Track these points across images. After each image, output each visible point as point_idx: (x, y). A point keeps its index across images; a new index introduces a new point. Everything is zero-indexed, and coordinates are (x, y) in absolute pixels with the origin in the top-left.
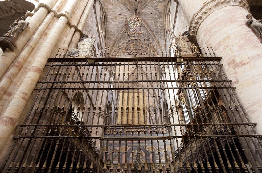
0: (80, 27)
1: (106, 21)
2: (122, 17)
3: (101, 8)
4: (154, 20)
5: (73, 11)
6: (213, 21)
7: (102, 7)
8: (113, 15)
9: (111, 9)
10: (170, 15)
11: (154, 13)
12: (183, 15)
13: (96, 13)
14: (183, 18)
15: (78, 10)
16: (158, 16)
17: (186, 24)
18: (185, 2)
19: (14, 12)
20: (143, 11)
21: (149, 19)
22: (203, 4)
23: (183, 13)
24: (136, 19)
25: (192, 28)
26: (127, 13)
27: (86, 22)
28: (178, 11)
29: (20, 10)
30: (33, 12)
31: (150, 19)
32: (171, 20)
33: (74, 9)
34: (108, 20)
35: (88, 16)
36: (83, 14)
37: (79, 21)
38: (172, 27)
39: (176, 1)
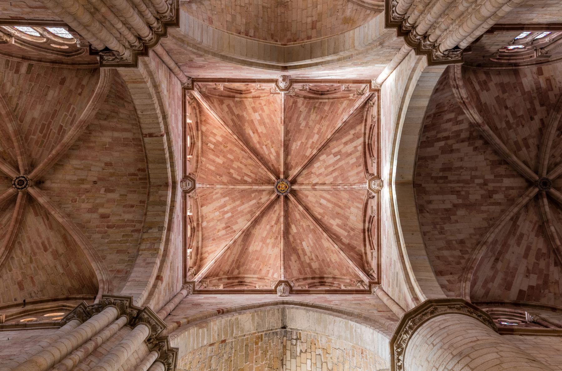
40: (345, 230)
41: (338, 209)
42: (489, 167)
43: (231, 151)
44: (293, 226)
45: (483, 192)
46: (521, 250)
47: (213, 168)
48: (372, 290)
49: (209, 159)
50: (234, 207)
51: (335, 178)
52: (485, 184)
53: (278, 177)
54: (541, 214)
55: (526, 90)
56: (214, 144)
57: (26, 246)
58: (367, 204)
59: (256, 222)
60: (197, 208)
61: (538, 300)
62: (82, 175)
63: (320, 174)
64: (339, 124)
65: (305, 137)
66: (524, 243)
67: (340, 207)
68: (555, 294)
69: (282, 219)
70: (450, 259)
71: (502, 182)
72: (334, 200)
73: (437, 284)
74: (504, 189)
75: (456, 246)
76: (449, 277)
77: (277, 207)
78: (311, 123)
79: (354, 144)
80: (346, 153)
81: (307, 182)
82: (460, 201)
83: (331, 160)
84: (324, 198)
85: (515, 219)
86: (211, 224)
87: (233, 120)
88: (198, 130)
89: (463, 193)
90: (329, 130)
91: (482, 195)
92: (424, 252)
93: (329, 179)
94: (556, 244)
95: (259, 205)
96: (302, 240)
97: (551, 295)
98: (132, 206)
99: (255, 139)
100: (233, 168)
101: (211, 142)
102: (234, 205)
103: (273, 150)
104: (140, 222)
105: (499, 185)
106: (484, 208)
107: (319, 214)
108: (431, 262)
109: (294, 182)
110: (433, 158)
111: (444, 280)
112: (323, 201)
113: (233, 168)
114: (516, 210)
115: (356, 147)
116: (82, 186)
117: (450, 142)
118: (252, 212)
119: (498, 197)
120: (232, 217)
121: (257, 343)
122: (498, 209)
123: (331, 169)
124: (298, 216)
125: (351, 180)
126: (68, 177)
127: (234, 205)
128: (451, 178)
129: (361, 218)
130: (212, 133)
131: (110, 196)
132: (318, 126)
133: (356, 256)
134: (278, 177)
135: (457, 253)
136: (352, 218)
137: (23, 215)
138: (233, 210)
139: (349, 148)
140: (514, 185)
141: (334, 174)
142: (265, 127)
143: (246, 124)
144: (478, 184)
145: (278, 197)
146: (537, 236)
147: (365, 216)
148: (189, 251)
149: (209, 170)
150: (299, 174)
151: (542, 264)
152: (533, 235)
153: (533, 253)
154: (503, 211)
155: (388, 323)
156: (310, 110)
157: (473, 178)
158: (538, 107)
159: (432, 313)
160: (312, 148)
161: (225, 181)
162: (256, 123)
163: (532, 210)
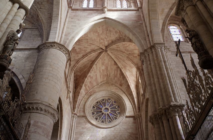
6: (43, 123)
42: (111, 39)
45: (103, 38)
46: (86, 46)
52: (106, 38)
55: (134, 51)
66: (88, 47)
68: (75, 56)
71: (106, 41)
74: (104, 42)
82: (100, 34)
89: (103, 34)
91: (102, 38)
94: (88, 55)
97: (74, 55)
105: (106, 41)
106: (98, 38)
110: (114, 29)
117: (119, 33)
119: (102, 41)
122: (98, 41)
128: (107, 31)
144: (106, 37)
146: (91, 49)
151: (83, 52)
152: (91, 48)
153: (86, 49)
154: (98, 42)
157: (108, 36)
158: (128, 52)
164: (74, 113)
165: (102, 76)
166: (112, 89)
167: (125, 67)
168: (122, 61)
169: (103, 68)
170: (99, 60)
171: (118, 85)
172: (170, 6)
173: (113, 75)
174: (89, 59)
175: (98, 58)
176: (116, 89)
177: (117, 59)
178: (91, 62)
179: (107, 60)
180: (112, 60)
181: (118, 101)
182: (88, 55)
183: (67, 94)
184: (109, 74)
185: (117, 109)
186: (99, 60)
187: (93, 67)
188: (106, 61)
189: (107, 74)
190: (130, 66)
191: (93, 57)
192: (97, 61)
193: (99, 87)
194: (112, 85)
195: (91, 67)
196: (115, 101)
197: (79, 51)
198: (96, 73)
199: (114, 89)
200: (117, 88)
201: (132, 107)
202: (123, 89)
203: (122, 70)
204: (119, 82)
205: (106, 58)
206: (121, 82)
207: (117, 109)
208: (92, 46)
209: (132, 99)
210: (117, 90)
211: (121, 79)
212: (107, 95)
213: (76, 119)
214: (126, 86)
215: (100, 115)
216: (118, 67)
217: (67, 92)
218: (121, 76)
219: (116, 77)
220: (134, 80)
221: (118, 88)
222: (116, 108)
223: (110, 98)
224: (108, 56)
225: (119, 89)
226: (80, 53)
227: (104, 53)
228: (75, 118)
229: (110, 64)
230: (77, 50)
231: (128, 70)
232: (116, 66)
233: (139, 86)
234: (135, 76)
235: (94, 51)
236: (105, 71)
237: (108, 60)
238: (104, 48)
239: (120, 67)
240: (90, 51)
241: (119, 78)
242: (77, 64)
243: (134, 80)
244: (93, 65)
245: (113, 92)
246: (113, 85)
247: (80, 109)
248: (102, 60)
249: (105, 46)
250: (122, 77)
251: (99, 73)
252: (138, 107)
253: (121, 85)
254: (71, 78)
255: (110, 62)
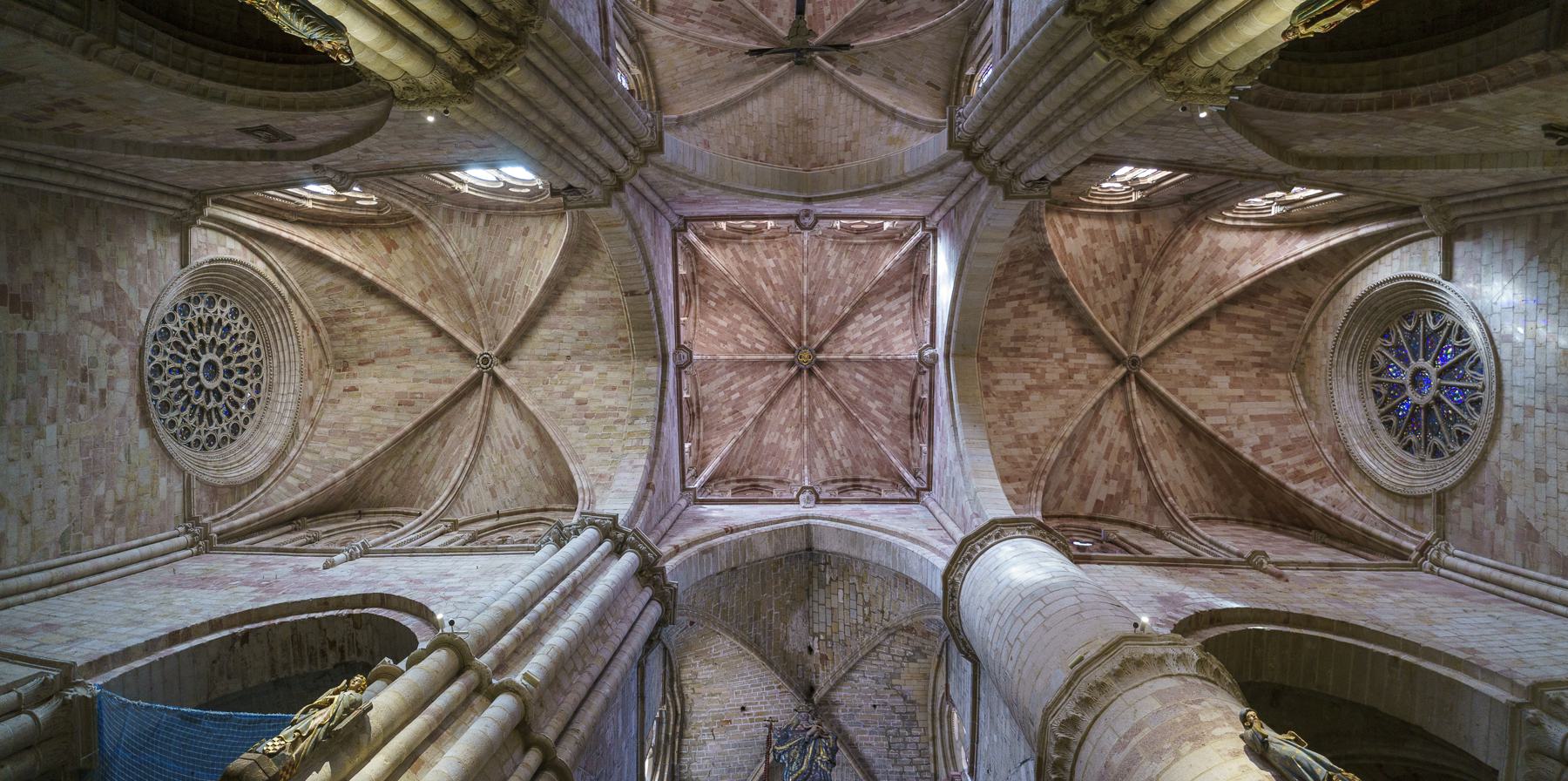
0: (565, 754)
1: (682, 736)
2: (752, 720)
3: (668, 674)
4: (888, 736)
5: (556, 677)
7: (671, 670)
8: (715, 708)
9: (709, 682)
10: (950, 716)
11: (885, 704)
12: (1004, 710)
13: (642, 697)
14: (1006, 727)
15: (576, 677)
16: (903, 718)
17: (1023, 750)
18: (1004, 659)
19: (333, 658)
20: (838, 696)
21: (864, 732)
22: (1072, 667)
23: (1002, 705)
24: (809, 733)
25: (1049, 768)
26: (773, 703)
27: (596, 729)
28: (983, 695)
29: (359, 652)
30: (402, 665)
31: (871, 733)
32: (956, 737)
33: (563, 668)
34: (690, 731)
35: (609, 701)
36: (593, 694)
37: (570, 723)
38: (965, 765)
39: (966, 657)
40: (886, 415)
41: (878, 388)
43: (737, 310)
44: (819, 410)
46: (1101, 449)
47: (714, 333)
48: (921, 499)
49: (711, 322)
50: (743, 386)
51: (875, 346)
53: (800, 344)
54: (1127, 403)
56: (716, 301)
57: (496, 441)
58: (916, 381)
59: (771, 405)
60: (696, 387)
61: (1116, 513)
62: (553, 347)
63: (856, 340)
64: (881, 273)
65: (834, 290)
66: (1106, 439)
67: (880, 384)
69: (805, 401)
70: (1020, 460)
72: (873, 375)
73: (1003, 496)
75: (1028, 442)
76: (1018, 484)
77: (798, 384)
78: (842, 272)
79: (901, 300)
80: (890, 311)
81: (838, 350)
83: (871, 320)
84: (861, 372)
85: (1097, 407)
86: (715, 408)
87: (739, 269)
88: (694, 283)
90: (868, 281)
92: (988, 452)
93: (868, 346)
95: (775, 381)
96: (830, 429)
98: (614, 388)
99: (769, 292)
100: (741, 333)
101: (711, 298)
102: (743, 382)
103: (792, 307)
104: (624, 409)
107: (854, 393)
108: (996, 464)
109: (819, 349)
111: (1011, 487)
112: (859, 377)
113: (741, 333)
114: (1099, 395)
115: (902, 304)
116: (555, 363)
118: (765, 392)
120: (740, 398)
121: (775, 570)
123: (870, 332)
124: (825, 397)
125: (896, 348)
126: (538, 352)
127: (743, 382)
129: (907, 399)
130: (713, 286)
131: (587, 374)
132: (851, 275)
133: (900, 451)
134: (800, 344)
135: (1028, 452)
136: (896, 399)
137: (490, 400)
138: (742, 389)
139: (894, 305)
140: (1099, 362)
141: (874, 341)
142: (783, 277)
143: (757, 274)
145: (800, 371)
146: (1121, 430)
147: (913, 397)
148: (687, 446)
149: (710, 335)
150: (827, 340)
151: (1125, 466)
152: (1117, 428)
153: (1115, 453)
155: (942, 546)
156: (841, 254)
159: (997, 537)
160: (844, 304)
161: (731, 350)
162: (770, 272)
163: (1118, 397)
164: (1414, 556)
165: (1264, 392)
166: (1326, 345)
167: (1215, 282)
168: (1187, 295)
169: (1222, 381)
170: (1183, 399)
171: (1309, 318)
172: (884, 119)
173: (1257, 338)
174: (1175, 445)
175: (1171, 402)
176: (1325, 328)
177: (1177, 314)
178: (1191, 434)
179: (1184, 361)
180: (1183, 339)
181: (1380, 320)
182: (1143, 447)
183: (1265, 571)
184: (1258, 359)
185: (1418, 324)
186: (1183, 399)
187: (1210, 428)
188: (1191, 365)
189: (1255, 365)
190: (1212, 257)
191: (1168, 425)
192: (1183, 407)
193: (1316, 410)
194: (1306, 345)
195: (1210, 438)
196: (1384, 336)
197: (1116, 482)
198: (1247, 418)
199: (1325, 339)
200: (1320, 322)
201: (1405, 248)
202: (1325, 294)
203: (1227, 294)
204: (1290, 311)
205: (1173, 367)
206: (1292, 303)
207: (1418, 324)
208: (1108, 425)
209: (1368, 247)
210: (1330, 323)
211: (1274, 301)
212: (1354, 374)
213: (1451, 549)
214: (1310, 281)
215: (1446, 418)
216: (1219, 310)
217: (1253, 573)
218: (1259, 302)
219: (1268, 328)
220: (1280, 242)
221: (1321, 318)
222: (1412, 332)
223: (1369, 360)
224: (1167, 355)
225: (1324, 315)
226: (1129, 482)
227: (1149, 371)
228: (1444, 555)
229: (1205, 351)
230: (1113, 492)
231: (1228, 268)
232: (1216, 326)
233: (1308, 219)
234: (1258, 235)
235: (1128, 421)
236: (1239, 374)
237: (1182, 356)
238: (1121, 371)
239: (1215, 302)
240: (1126, 435)
241: (1272, 311)
242: (1166, 498)
243: (1280, 242)
244: (1203, 428)
245: (1339, 343)
246: (1309, 341)
247: (1406, 520)
248: (1182, 384)
249: (1113, 367)
250: (1263, 298)
251: (1246, 404)
252: (1399, 219)
253: (1307, 303)
254: (1211, 542)
255: (1196, 351)
